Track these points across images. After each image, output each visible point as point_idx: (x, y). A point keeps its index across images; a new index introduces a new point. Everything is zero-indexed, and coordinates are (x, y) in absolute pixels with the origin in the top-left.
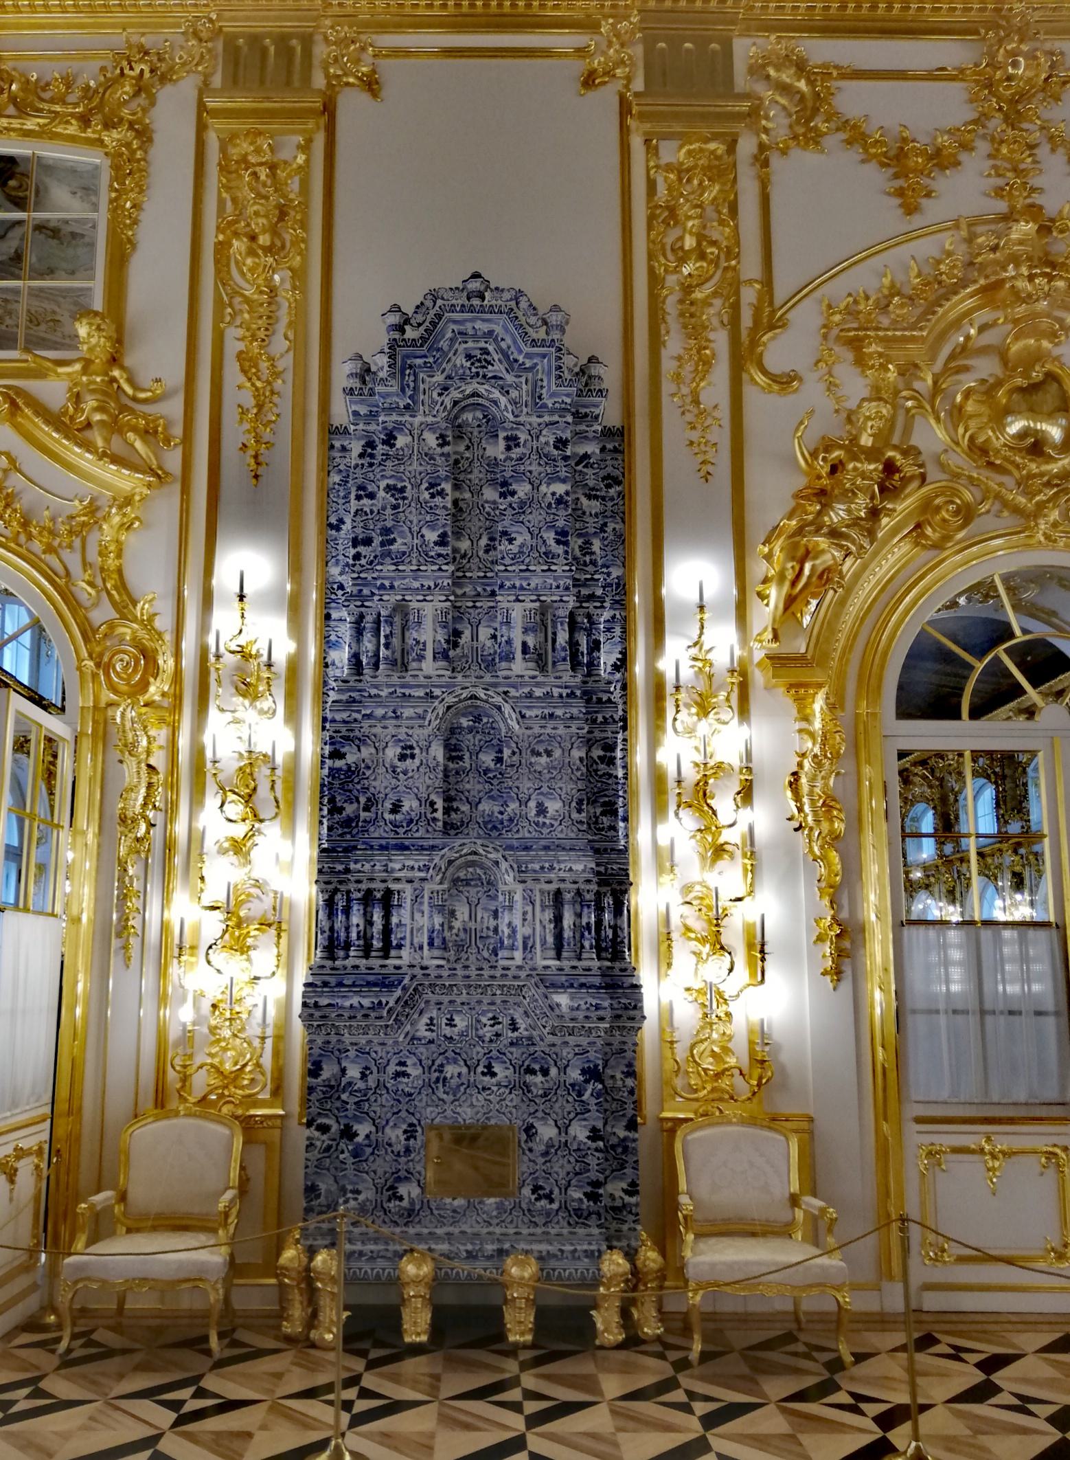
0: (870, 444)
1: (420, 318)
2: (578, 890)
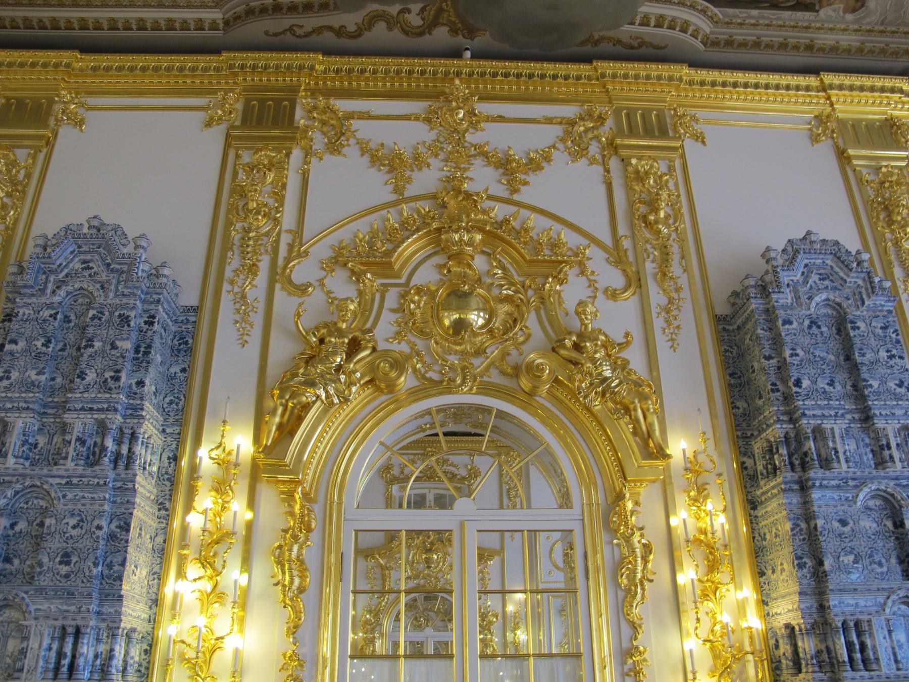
1: (54, 242)
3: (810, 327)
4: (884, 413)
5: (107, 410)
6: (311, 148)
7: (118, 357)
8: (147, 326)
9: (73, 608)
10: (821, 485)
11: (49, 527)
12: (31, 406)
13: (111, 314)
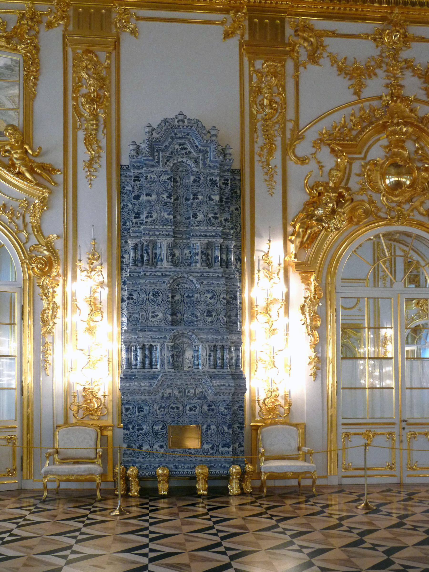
0: (333, 186)
2: (223, 346)
5: (215, 236)
6: (298, 59)
7: (214, 205)
8: (224, 186)
9: (220, 337)
11: (197, 298)
12: (170, 234)
13: (205, 178)
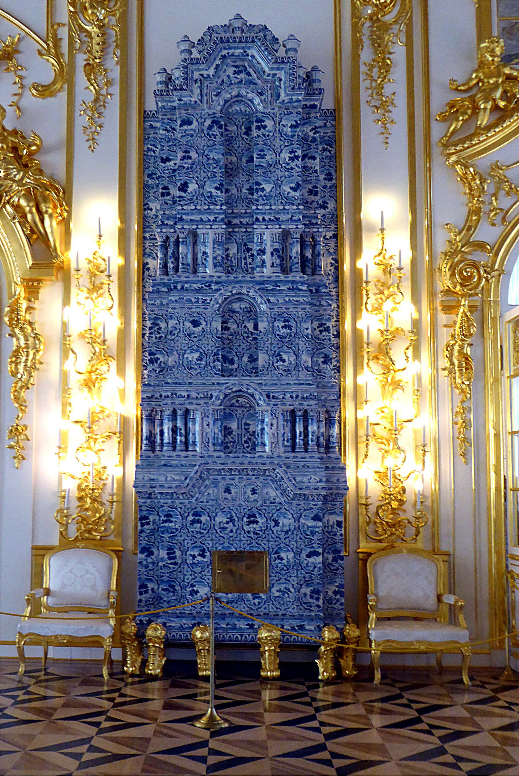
3: (210, 127)
4: (267, 218)
10: (182, 288)
